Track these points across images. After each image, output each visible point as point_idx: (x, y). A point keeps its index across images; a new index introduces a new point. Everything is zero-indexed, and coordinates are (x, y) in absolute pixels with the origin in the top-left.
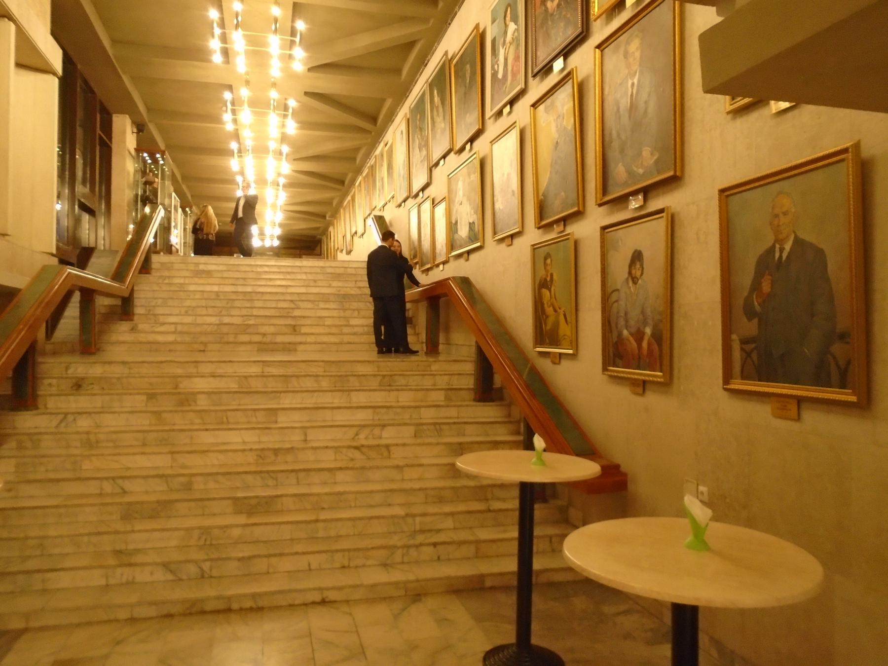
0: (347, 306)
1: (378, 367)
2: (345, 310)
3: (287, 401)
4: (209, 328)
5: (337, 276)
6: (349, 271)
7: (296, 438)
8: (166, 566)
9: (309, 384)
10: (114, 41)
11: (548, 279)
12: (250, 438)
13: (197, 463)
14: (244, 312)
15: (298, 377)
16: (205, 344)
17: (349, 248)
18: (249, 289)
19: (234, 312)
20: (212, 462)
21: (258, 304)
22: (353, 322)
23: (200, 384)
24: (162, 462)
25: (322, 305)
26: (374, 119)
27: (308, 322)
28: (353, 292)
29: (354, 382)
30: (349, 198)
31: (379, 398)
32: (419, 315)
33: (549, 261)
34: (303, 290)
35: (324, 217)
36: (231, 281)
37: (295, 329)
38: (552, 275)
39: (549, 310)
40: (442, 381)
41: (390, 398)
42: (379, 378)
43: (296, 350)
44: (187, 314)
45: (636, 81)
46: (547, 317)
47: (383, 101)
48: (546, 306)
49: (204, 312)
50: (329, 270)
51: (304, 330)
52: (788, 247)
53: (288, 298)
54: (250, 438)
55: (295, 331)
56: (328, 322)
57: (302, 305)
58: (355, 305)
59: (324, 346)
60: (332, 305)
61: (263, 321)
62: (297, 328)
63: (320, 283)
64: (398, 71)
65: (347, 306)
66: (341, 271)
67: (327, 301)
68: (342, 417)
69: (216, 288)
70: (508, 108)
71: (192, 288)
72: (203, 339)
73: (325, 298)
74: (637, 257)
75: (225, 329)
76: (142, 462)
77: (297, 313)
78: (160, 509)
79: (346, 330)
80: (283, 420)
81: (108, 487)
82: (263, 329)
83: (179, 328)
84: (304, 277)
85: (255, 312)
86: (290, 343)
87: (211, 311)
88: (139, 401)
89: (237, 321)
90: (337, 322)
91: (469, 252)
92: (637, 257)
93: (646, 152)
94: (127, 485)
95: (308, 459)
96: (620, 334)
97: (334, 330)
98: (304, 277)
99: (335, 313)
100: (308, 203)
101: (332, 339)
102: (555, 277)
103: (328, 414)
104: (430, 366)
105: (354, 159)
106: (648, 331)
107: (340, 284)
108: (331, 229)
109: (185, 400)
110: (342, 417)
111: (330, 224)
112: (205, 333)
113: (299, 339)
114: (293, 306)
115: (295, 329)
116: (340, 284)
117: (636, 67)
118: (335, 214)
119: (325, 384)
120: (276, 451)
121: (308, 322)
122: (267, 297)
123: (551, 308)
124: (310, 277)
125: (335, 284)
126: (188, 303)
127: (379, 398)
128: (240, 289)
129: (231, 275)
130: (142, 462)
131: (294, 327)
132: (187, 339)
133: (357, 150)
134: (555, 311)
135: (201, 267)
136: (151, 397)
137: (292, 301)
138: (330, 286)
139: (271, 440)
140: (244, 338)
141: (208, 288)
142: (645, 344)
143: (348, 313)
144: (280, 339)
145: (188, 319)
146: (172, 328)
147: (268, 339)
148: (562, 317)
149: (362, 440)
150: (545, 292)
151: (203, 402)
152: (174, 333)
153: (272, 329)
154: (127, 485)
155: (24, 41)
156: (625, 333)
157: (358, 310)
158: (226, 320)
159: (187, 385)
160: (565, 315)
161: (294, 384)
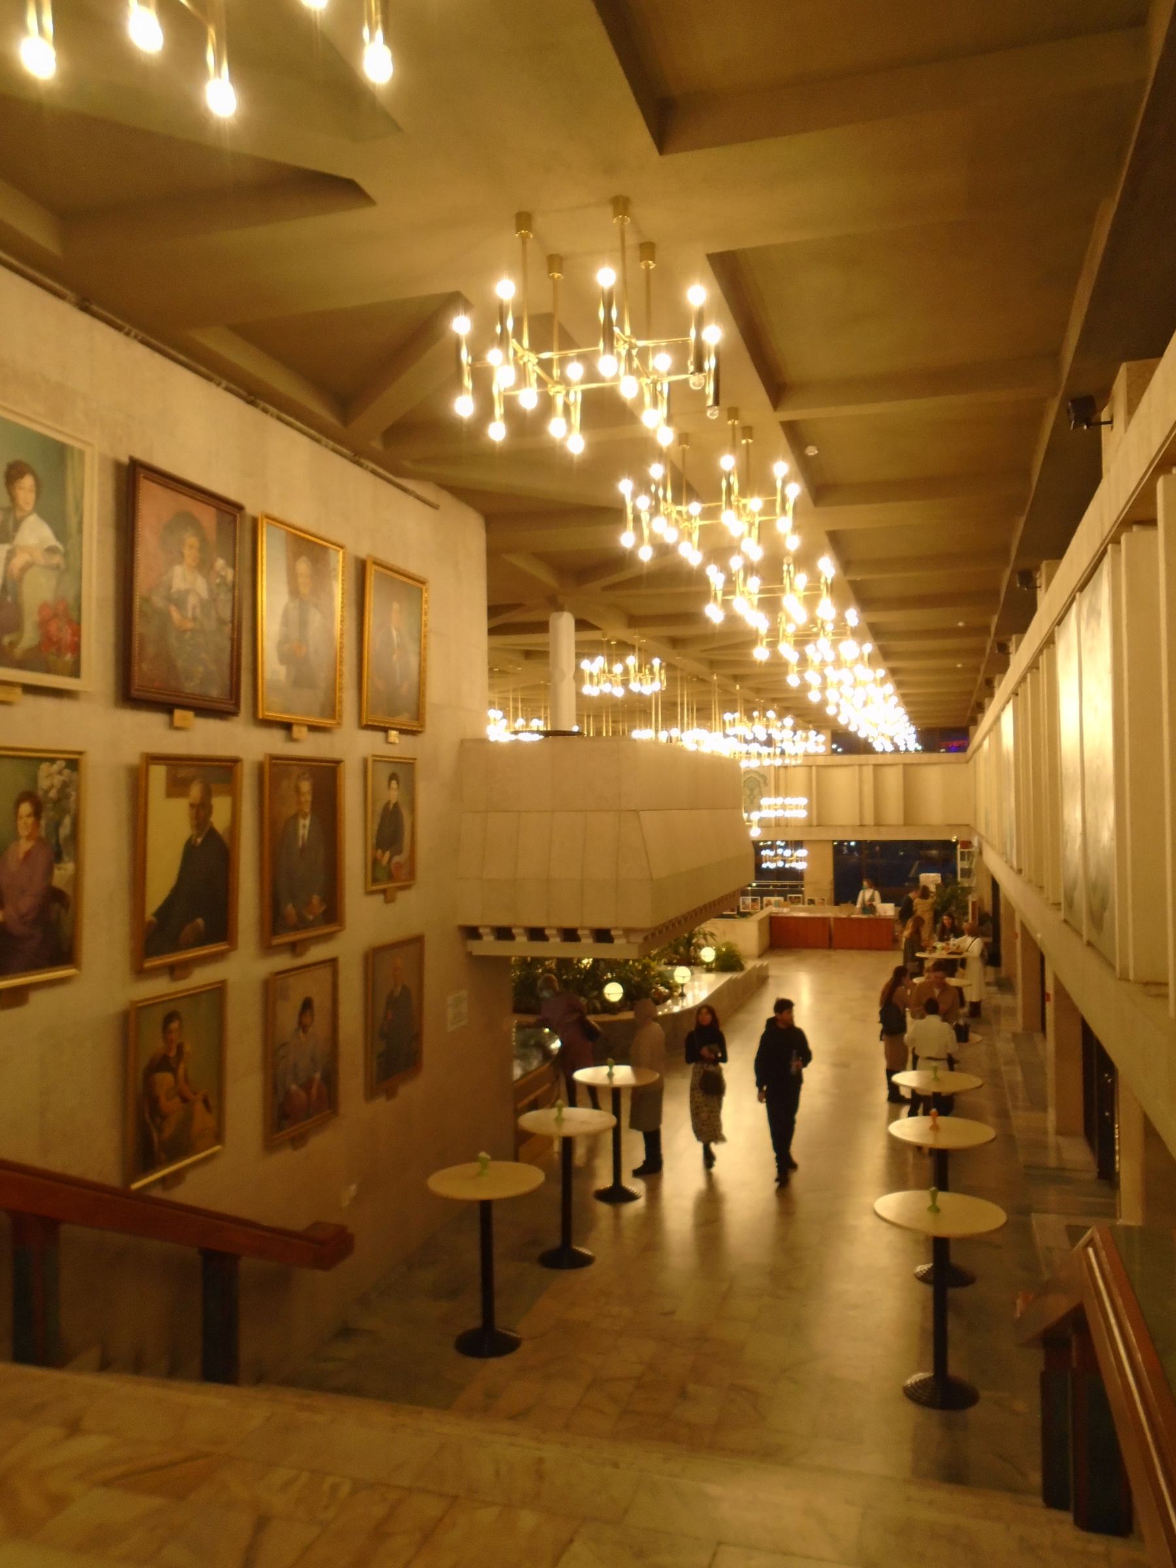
11: (173, 1053)
33: (174, 1025)
38: (180, 1048)
39: (171, 1105)
45: (307, 822)
46: (164, 1118)
48: (163, 1100)
52: (399, 988)
74: (307, 1004)
92: (307, 1004)
93: (316, 899)
96: (288, 1093)
102: (188, 1048)
106: (318, 1076)
117: (307, 809)
123: (177, 1100)
134: (185, 1100)
142: (314, 1091)
148: (199, 1106)
150: (164, 1079)
156: (294, 1087)
160: (206, 1102)
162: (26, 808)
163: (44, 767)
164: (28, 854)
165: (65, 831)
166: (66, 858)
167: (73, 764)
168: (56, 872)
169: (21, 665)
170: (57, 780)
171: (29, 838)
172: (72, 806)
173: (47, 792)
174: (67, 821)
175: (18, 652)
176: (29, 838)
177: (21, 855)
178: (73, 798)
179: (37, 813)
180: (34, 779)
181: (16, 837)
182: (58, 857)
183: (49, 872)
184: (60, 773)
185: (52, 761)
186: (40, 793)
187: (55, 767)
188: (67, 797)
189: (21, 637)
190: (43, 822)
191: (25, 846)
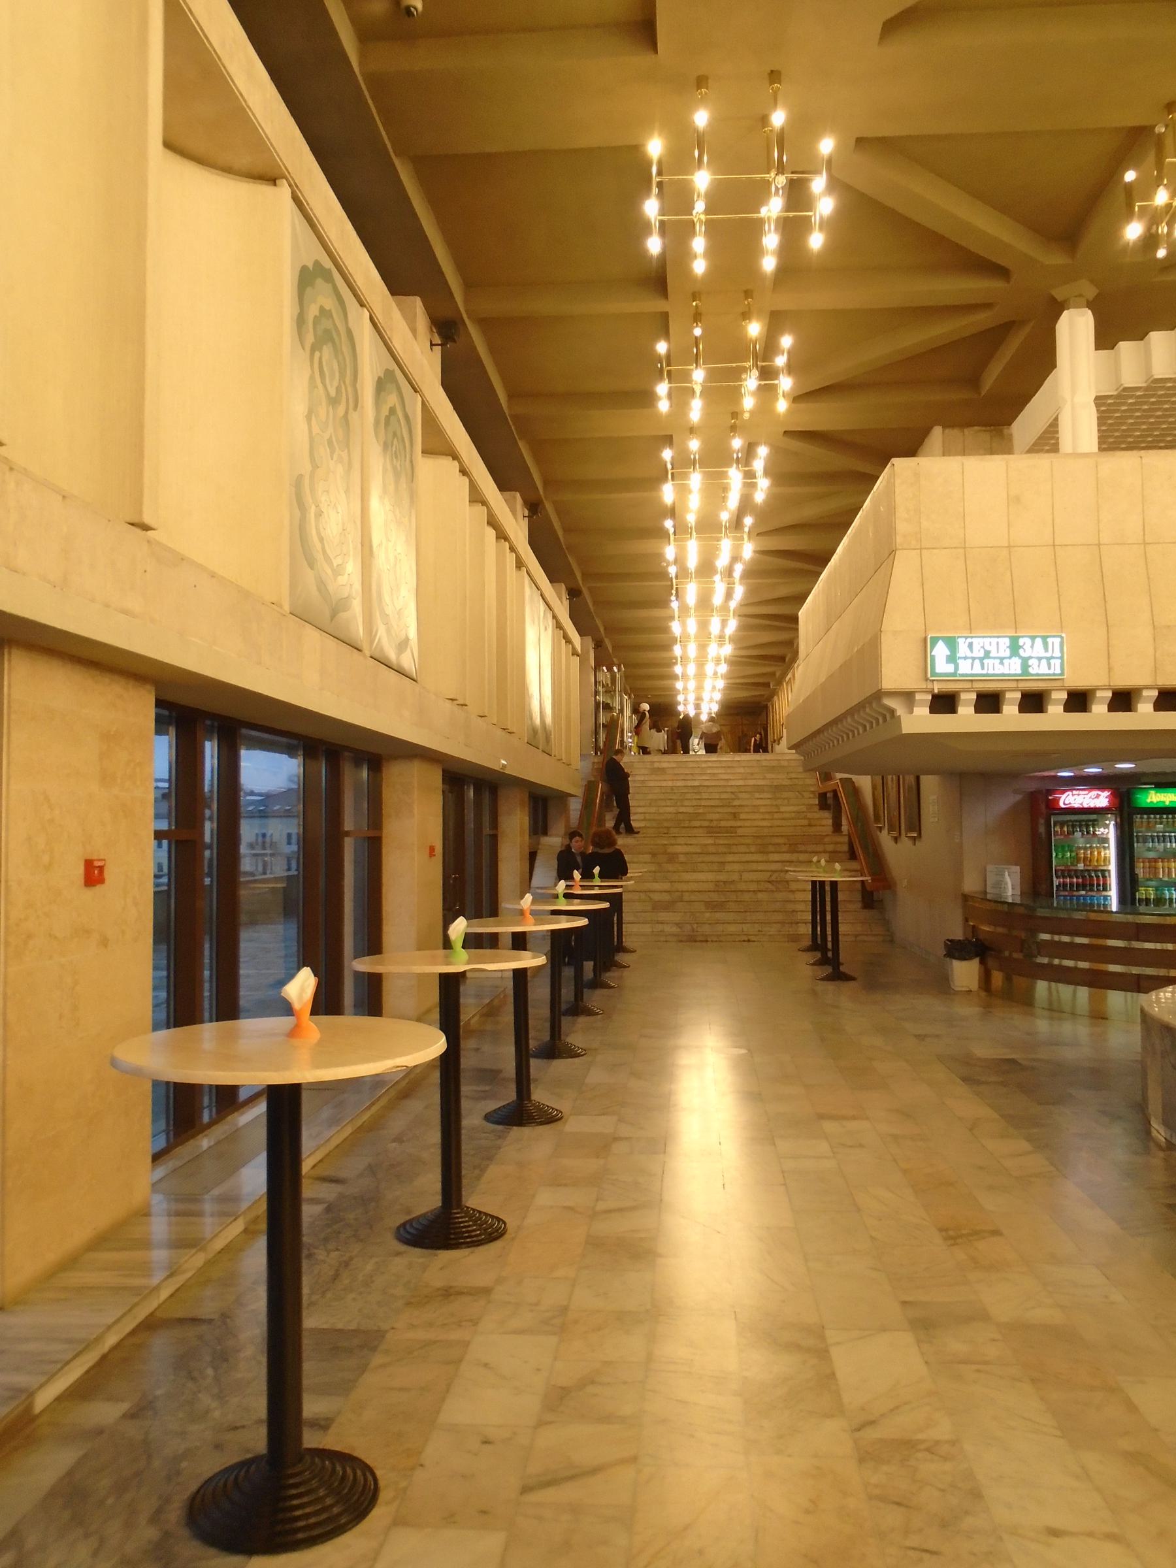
2: (776, 799)
3: (730, 858)
4: (669, 816)
5: (772, 769)
7: (735, 877)
8: (677, 924)
9: (743, 849)
10: (594, 603)
12: (711, 876)
13: (684, 887)
14: (695, 803)
16: (668, 828)
18: (696, 783)
19: (686, 803)
20: (693, 886)
21: (705, 796)
22: (783, 809)
23: (678, 849)
24: (666, 886)
25: (757, 795)
27: (746, 810)
29: (771, 848)
31: (787, 857)
32: (830, 801)
34: (741, 783)
35: (768, 685)
36: (682, 777)
37: (735, 816)
40: (830, 848)
41: (794, 857)
44: (650, 805)
49: (663, 803)
51: (742, 816)
53: (729, 790)
54: (711, 876)
56: (762, 810)
57: (741, 795)
58: (785, 795)
68: (761, 867)
69: (670, 784)
71: (652, 784)
72: (666, 824)
73: (759, 789)
75: (681, 817)
76: (657, 886)
77: (736, 803)
78: (667, 906)
79: (776, 816)
80: (728, 867)
81: (643, 896)
82: (710, 817)
83: (647, 817)
84: (741, 770)
85: (703, 803)
87: (669, 803)
88: (647, 858)
89: (690, 810)
94: (652, 895)
95: (743, 886)
97: (767, 816)
98: (741, 770)
99: (768, 802)
100: (744, 677)
101: (765, 823)
103: (754, 866)
107: (773, 776)
108: (776, 698)
109: (672, 858)
110: (761, 867)
111: (774, 693)
112: (666, 820)
113: (739, 823)
115: (735, 816)
116: (773, 776)
118: (780, 683)
119: (753, 849)
120: (725, 882)
121: (746, 810)
122: (711, 790)
124: (748, 771)
125: (769, 776)
126: (650, 796)
127: (787, 857)
128: (690, 783)
129: (682, 771)
130: (657, 886)
131: (734, 814)
132: (655, 824)
135: (656, 765)
136: (654, 855)
139: (722, 877)
140: (698, 824)
141: (664, 784)
143: (779, 802)
144: (723, 824)
145: (653, 810)
146: (642, 817)
147: (714, 824)
149: (773, 878)
151: (682, 858)
152: (644, 820)
153: (717, 816)
154: (652, 895)
155: (574, 648)
158: (681, 810)
159: (671, 849)
161: (734, 849)
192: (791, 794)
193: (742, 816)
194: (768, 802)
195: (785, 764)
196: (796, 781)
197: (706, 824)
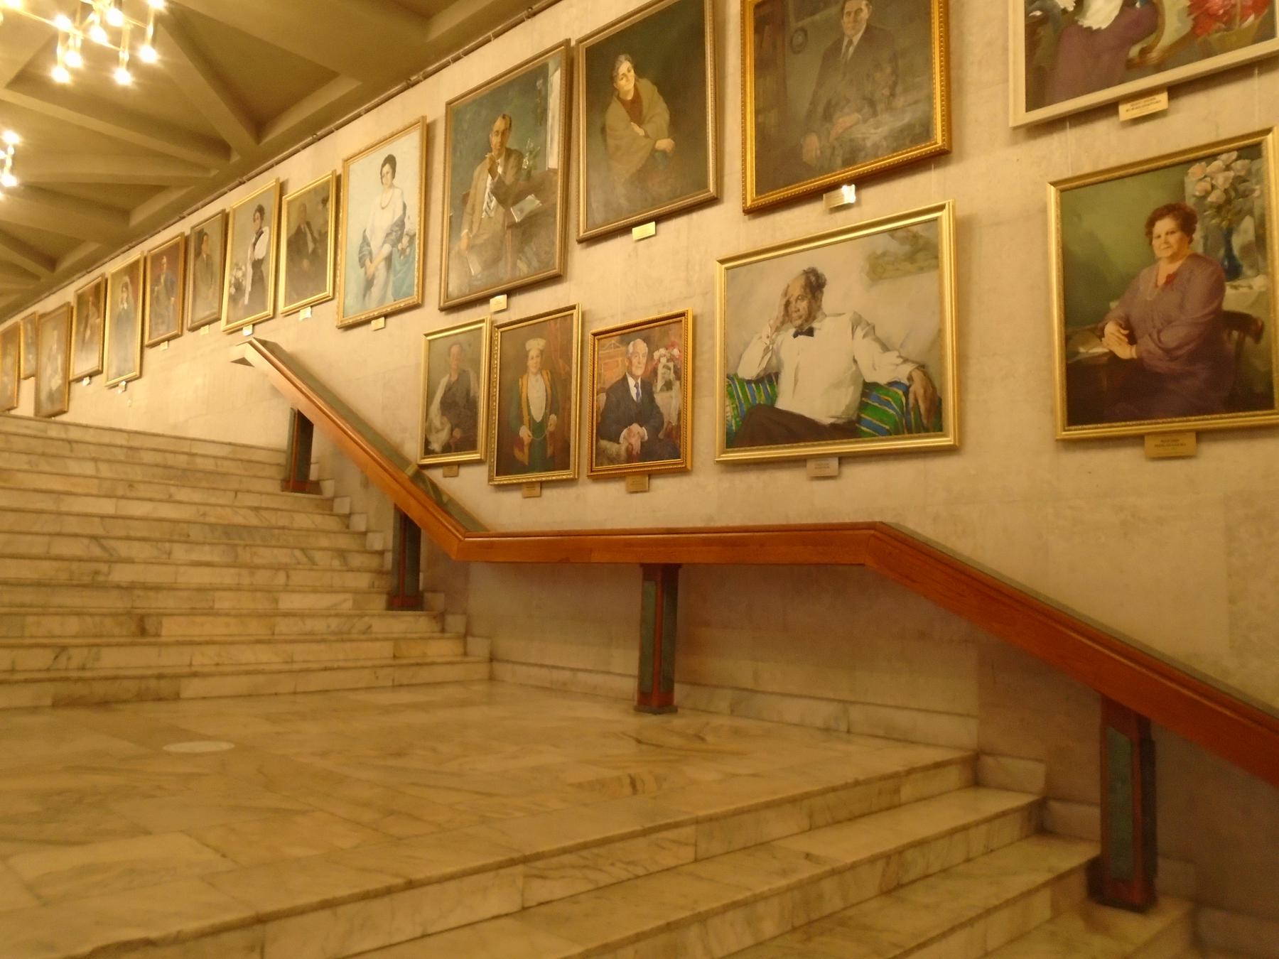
0: (245, 556)
1: (811, 816)
2: (253, 568)
6: (201, 463)
15: (701, 919)
17: (47, 408)
22: (290, 602)
25: (180, 552)
26: (259, 124)
28: (239, 520)
30: (68, 294)
34: (107, 507)
37: (142, 628)
42: (880, 865)
43: (177, 697)
47: (325, 77)
50: (148, 457)
55: (143, 632)
58: (266, 555)
59: (261, 679)
60: (206, 554)
61: (27, 596)
62: (150, 625)
63: (143, 491)
64: (424, 16)
65: (245, 556)
66: (182, 461)
67: (187, 541)
70: (1161, 101)
73: (176, 533)
77: (122, 574)
86: (160, 677)
90: (246, 602)
91: (843, 459)
104: (897, 791)
105: (125, 214)
113: (171, 660)
114: (97, 551)
115: (142, 628)
125: (182, 494)
133: (157, 189)
137: (94, 538)
138: (170, 500)
144: (111, 660)
157: (284, 568)
162: (1165, 225)
163: (1196, 170)
164: (1171, 279)
165: (1237, 242)
166: (1247, 271)
167: (1251, 150)
168: (1229, 291)
169: (1160, 67)
170: (1221, 180)
171: (1173, 258)
172: (1257, 204)
173: (1203, 198)
174: (1248, 224)
175: (1154, 55)
176: (1173, 258)
177: (1162, 280)
178: (1257, 194)
179: (1187, 222)
180: (1181, 186)
181: (1152, 260)
182: (1233, 272)
183: (1217, 292)
184: (1228, 168)
185: (1214, 157)
186: (1190, 203)
187: (1218, 164)
188: (1245, 195)
189: (1158, 39)
190: (1197, 236)
191: (1166, 269)
192: (282, 556)
193: (172, 629)
194: (228, 577)
195: (209, 465)
196: (273, 519)
197: (38, 660)
